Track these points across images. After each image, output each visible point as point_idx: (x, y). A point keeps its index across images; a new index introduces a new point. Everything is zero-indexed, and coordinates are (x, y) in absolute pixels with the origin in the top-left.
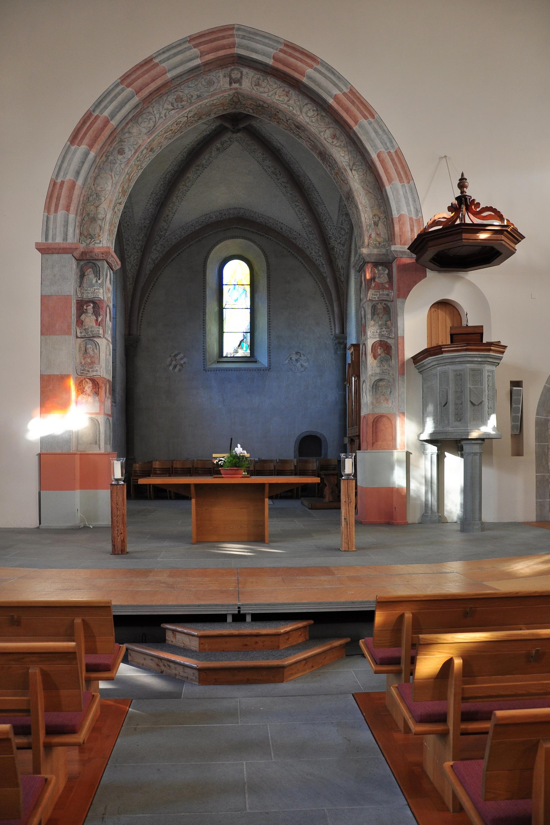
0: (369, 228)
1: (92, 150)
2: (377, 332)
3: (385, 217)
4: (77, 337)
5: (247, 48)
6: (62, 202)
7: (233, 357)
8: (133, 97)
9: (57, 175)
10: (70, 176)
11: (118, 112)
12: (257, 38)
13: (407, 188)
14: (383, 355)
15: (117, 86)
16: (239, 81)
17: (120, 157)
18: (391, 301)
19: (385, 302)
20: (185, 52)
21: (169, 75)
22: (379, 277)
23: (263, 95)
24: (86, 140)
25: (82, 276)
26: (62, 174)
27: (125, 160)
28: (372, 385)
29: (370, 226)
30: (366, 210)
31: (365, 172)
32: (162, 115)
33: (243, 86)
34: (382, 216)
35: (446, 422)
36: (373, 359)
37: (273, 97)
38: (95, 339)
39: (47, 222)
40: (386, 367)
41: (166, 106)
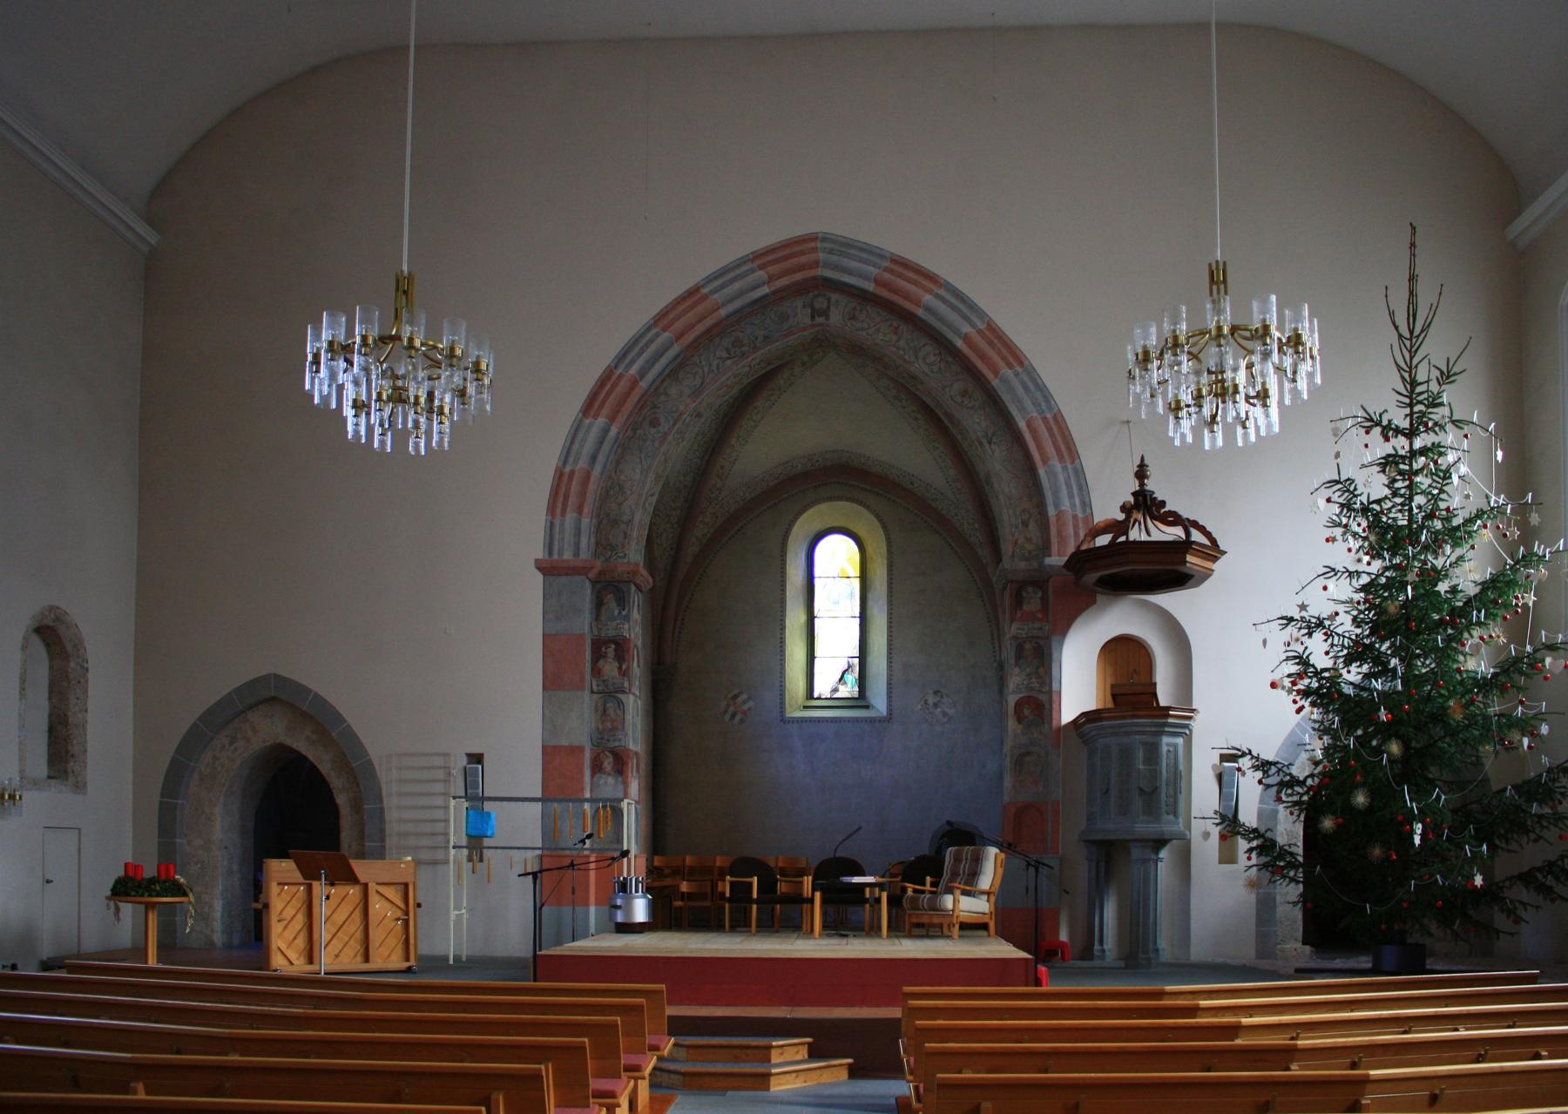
1: (614, 424)
3: (1040, 514)
4: (592, 692)
5: (836, 267)
6: (572, 500)
7: (831, 699)
8: (672, 344)
9: (565, 463)
10: (582, 464)
11: (650, 368)
12: (852, 252)
13: (1070, 471)
15: (649, 329)
16: (824, 313)
17: (653, 431)
20: (747, 275)
21: (723, 312)
23: (860, 333)
24: (606, 411)
25: (599, 604)
26: (571, 460)
27: (660, 435)
32: (714, 367)
33: (831, 321)
37: (876, 335)
38: (619, 696)
39: (551, 530)
41: (718, 354)
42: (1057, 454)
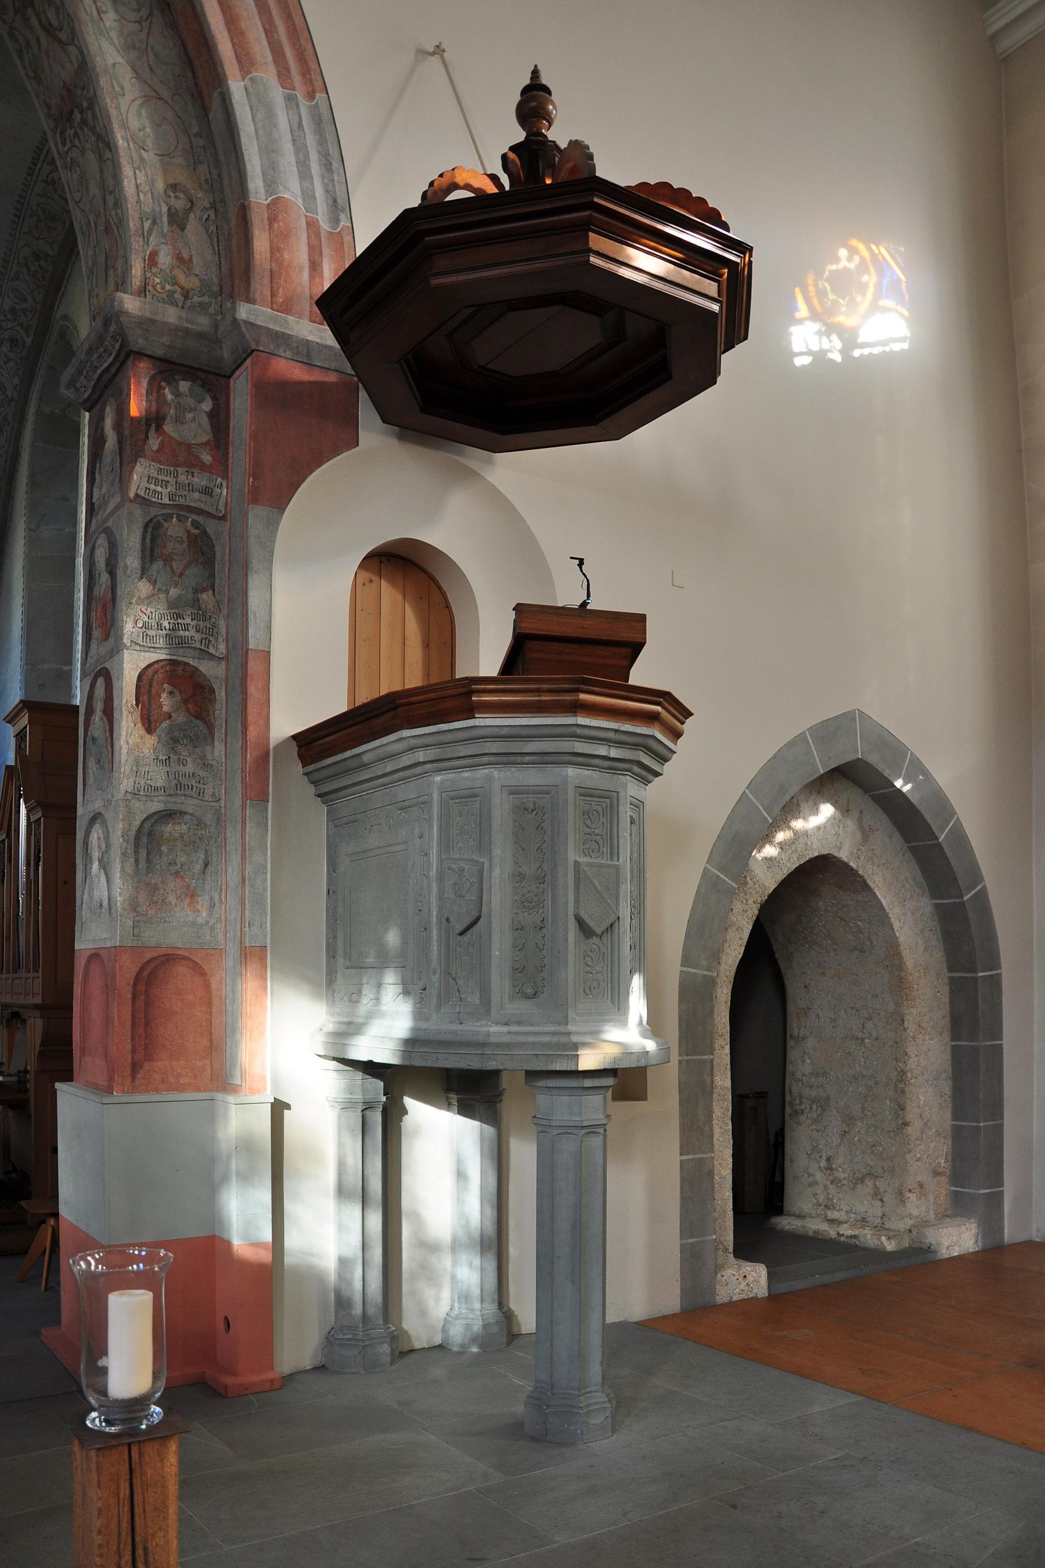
0: (150, 230)
2: (160, 627)
3: (213, 206)
13: (304, 111)
14: (180, 718)
18: (219, 518)
19: (194, 517)
22: (179, 420)
28: (133, 833)
29: (154, 222)
30: (141, 157)
31: (144, 12)
34: (203, 199)
35: (474, 999)
36: (142, 732)
40: (190, 767)
42: (275, 61)
